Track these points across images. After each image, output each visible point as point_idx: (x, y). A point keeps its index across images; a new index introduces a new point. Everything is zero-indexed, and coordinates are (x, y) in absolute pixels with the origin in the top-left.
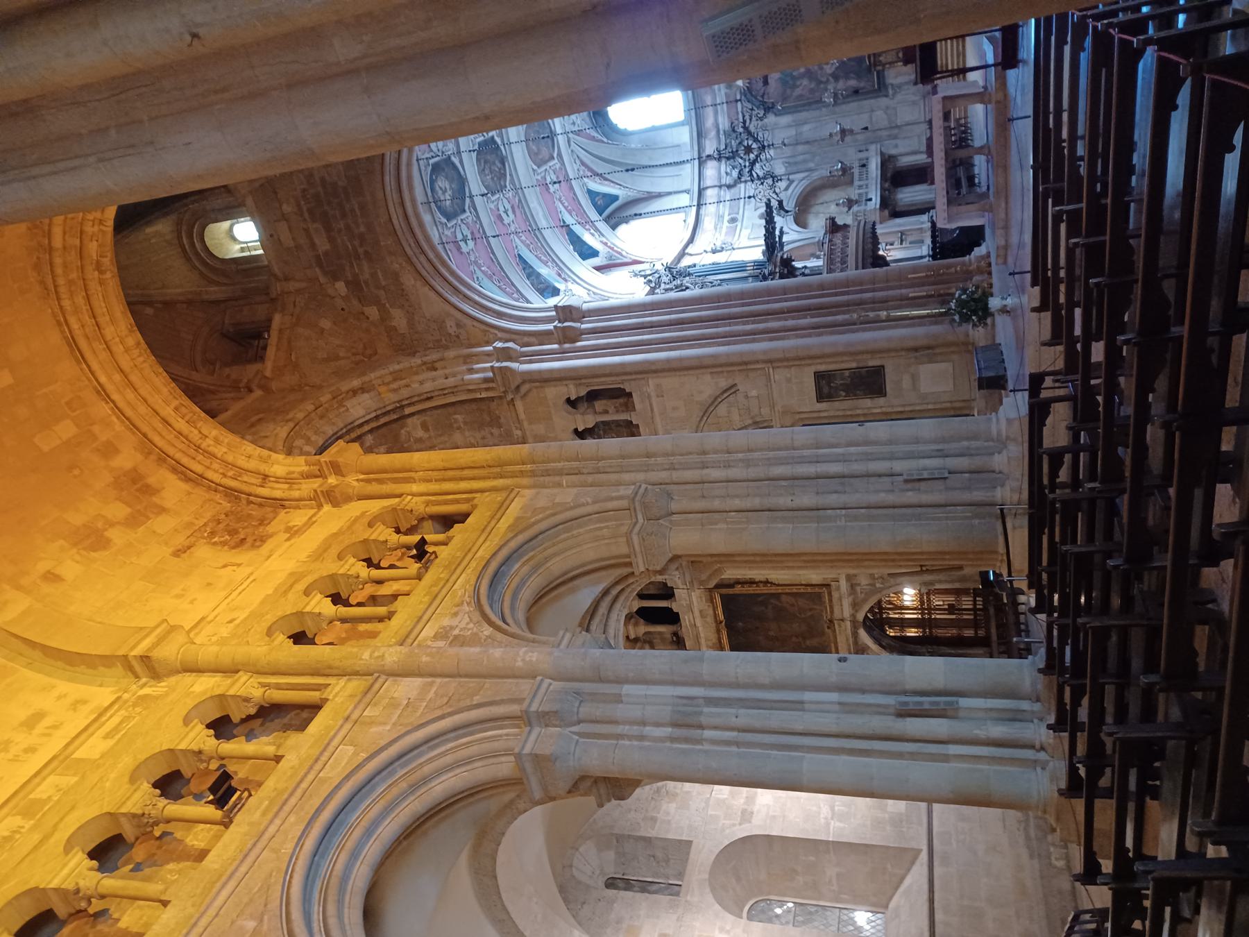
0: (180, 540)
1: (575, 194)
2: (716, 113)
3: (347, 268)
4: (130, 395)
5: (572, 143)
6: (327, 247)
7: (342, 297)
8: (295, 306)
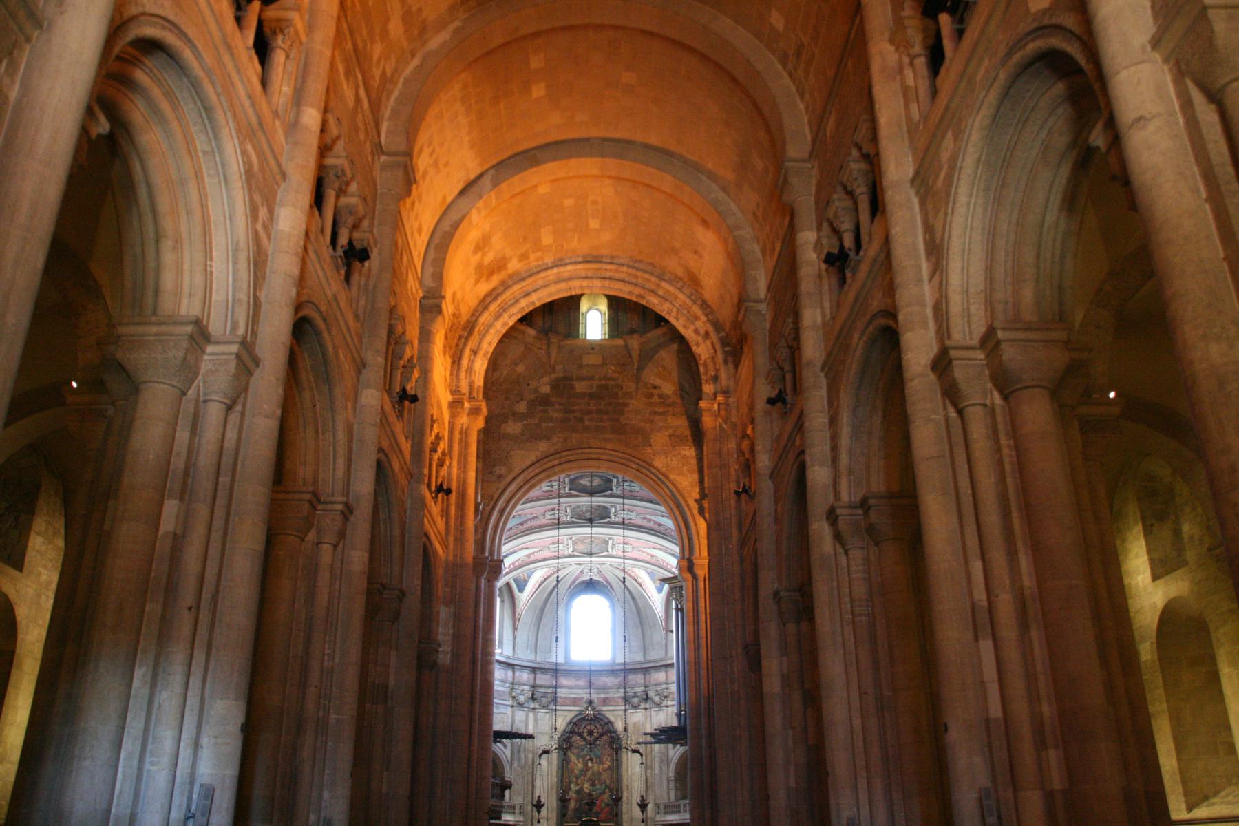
0: (459, 295)
1: (540, 561)
2: (570, 688)
3: (558, 399)
4: (551, 278)
5: (578, 566)
6: (578, 390)
7: (537, 388)
8: (539, 348)
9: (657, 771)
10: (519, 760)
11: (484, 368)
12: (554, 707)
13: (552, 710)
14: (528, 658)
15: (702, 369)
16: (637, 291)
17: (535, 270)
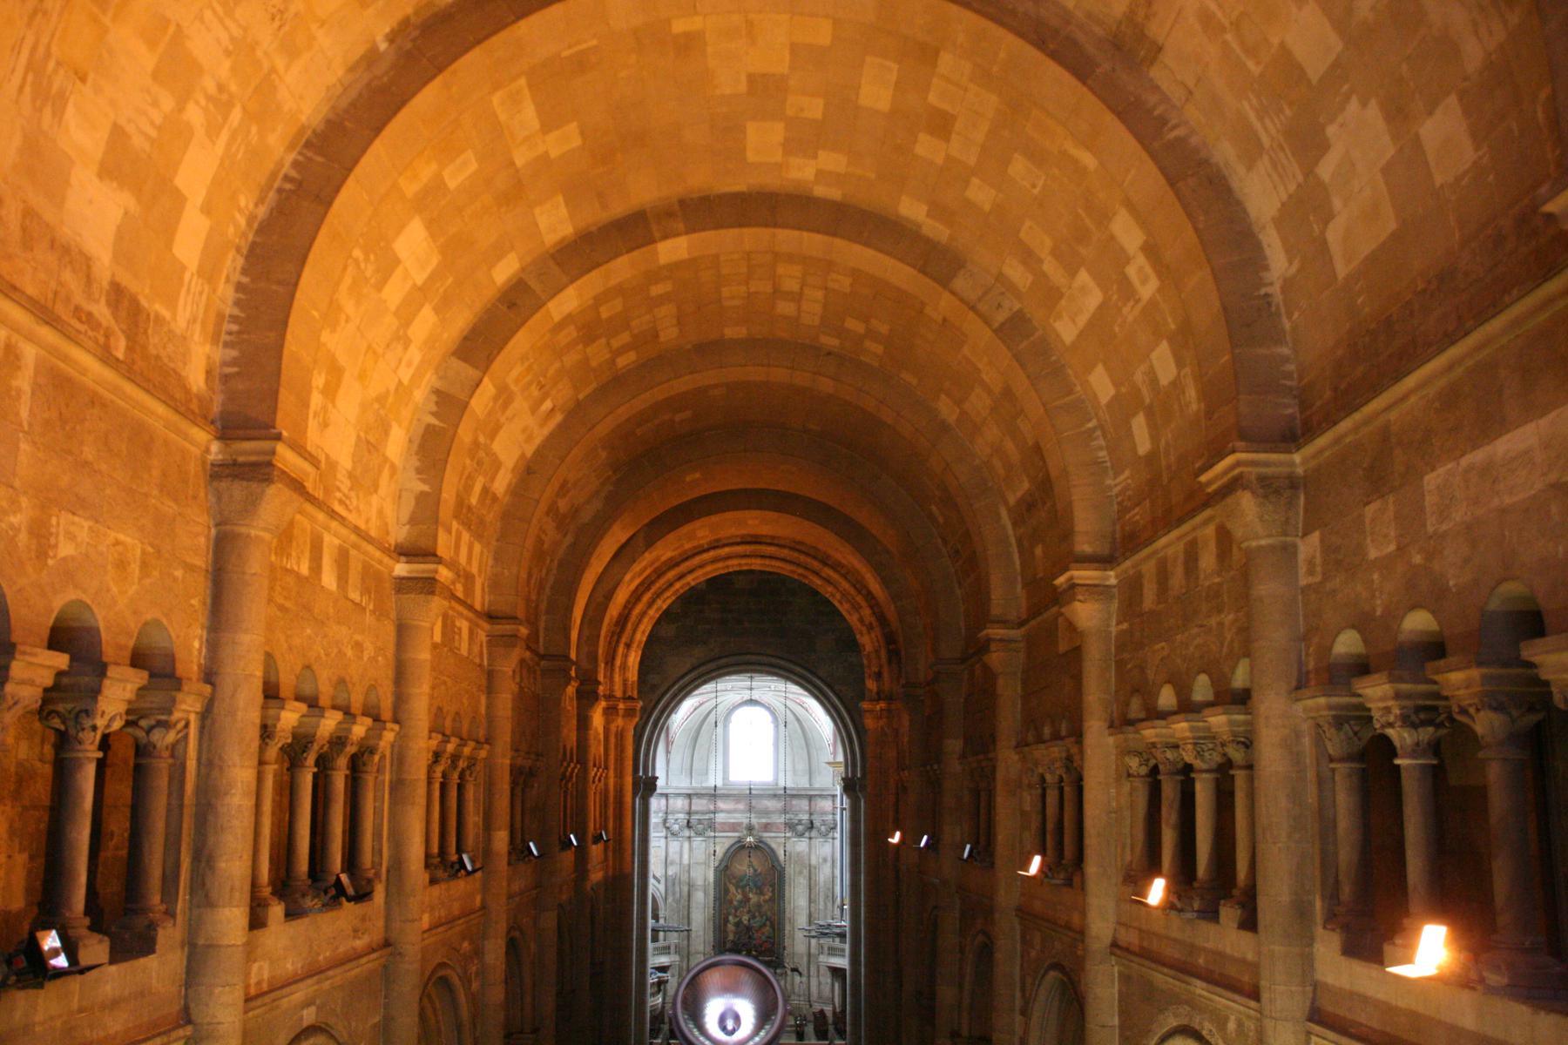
2: (729, 812)
9: (821, 907)
10: (674, 894)
11: (639, 659)
12: (712, 834)
13: (709, 837)
14: (683, 785)
15: (865, 662)
16: (800, 571)
17: (690, 553)
